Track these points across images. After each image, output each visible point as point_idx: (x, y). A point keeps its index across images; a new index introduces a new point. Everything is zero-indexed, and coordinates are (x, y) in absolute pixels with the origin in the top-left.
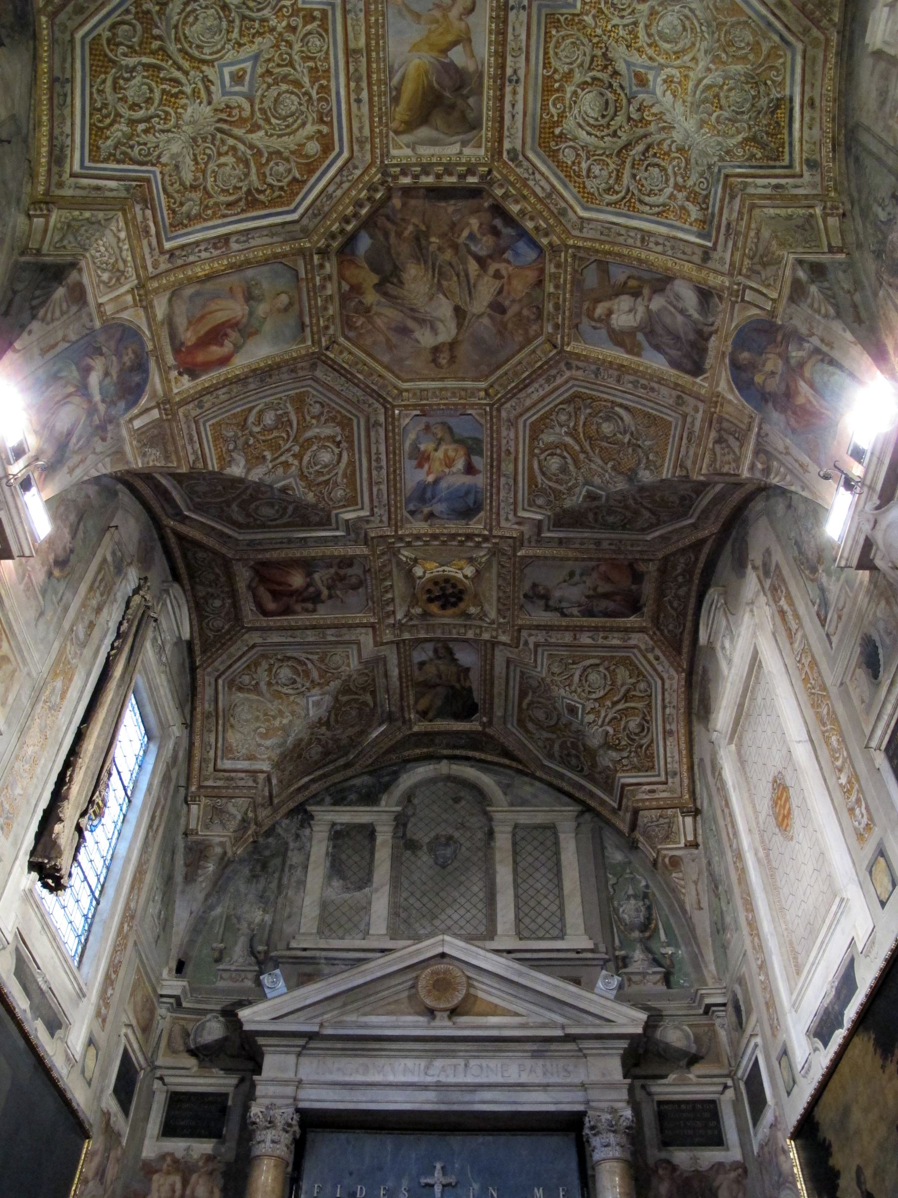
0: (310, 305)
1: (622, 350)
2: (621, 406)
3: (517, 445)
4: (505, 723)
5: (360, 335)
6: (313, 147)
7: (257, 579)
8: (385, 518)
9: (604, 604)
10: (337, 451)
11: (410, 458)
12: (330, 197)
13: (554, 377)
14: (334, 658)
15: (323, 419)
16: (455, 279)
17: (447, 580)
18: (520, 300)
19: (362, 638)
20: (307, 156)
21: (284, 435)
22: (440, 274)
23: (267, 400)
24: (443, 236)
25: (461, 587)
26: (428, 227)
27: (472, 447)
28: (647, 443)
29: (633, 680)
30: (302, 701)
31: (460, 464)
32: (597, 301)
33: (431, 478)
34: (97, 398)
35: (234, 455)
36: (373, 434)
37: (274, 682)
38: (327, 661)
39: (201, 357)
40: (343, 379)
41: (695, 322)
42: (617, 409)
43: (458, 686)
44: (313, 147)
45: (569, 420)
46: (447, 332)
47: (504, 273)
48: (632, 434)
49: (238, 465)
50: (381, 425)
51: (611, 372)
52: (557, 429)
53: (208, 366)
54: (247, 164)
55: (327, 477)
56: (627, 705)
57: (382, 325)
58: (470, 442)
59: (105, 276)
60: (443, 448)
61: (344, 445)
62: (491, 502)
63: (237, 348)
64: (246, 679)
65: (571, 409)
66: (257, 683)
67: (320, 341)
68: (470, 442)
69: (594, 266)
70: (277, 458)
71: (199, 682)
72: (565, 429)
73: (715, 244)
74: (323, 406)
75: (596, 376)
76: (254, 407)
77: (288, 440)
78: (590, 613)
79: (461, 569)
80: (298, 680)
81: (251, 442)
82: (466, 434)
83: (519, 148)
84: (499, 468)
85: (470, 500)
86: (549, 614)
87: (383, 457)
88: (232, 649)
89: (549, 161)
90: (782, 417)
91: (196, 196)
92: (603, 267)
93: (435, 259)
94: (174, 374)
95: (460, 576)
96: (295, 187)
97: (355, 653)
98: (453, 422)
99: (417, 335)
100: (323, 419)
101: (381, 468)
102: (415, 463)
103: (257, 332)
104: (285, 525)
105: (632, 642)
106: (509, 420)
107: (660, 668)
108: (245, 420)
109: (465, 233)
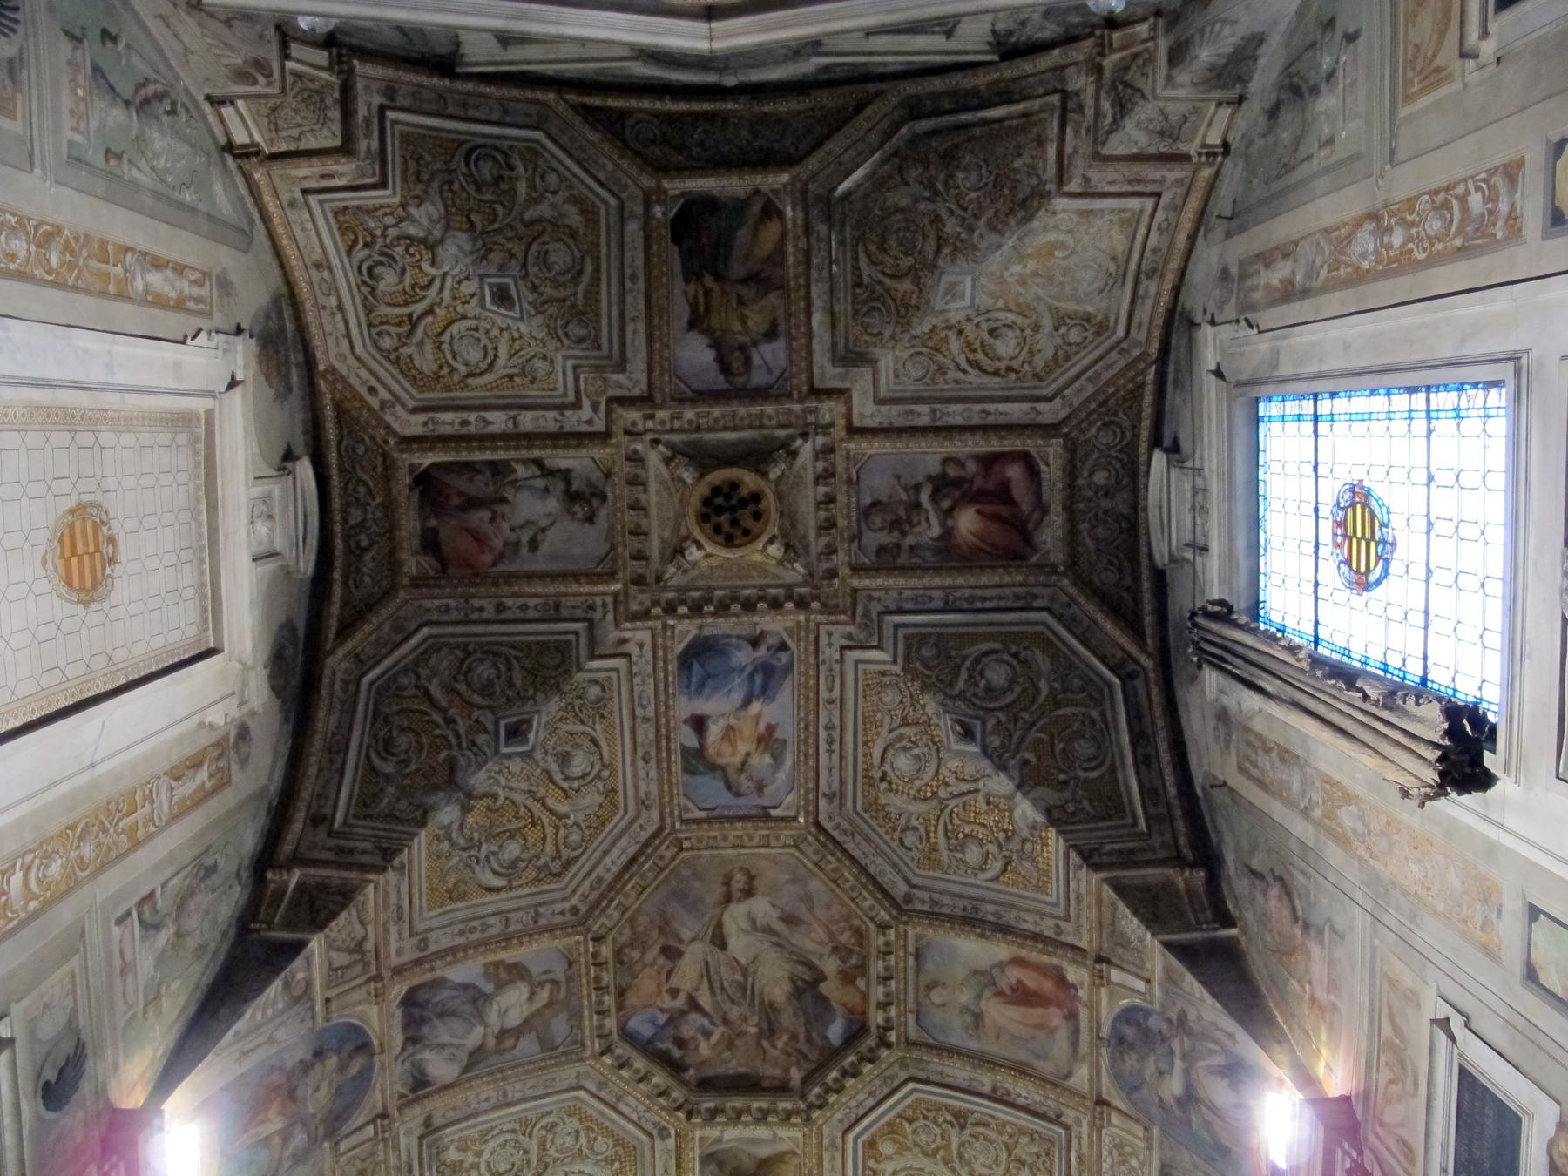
0: (906, 984)
2: (498, 890)
3: (635, 776)
4: (622, 207)
6: (886, 1148)
7: (1030, 526)
8: (824, 640)
9: (480, 486)
10: (887, 767)
11: (785, 742)
12: (872, 1094)
13: (592, 888)
14: (920, 374)
15: (903, 821)
16: (726, 984)
17: (729, 541)
18: (645, 966)
19: (870, 408)
20: (894, 1141)
21: (956, 821)
22: (743, 988)
23: (972, 881)
24: (741, 1034)
25: (708, 527)
26: (759, 1044)
27: (697, 760)
28: (456, 860)
29: (405, 351)
30: (984, 300)
31: (714, 731)
32: (549, 1005)
33: (755, 707)
34: (1178, 1063)
35: (1026, 833)
36: (836, 784)
37: (1028, 332)
38: (934, 367)
39: (1048, 986)
40: (872, 870)
41: (425, 1047)
42: (501, 882)
43: (709, 281)
44: (886, 1148)
45: (566, 837)
46: (735, 917)
47: (666, 997)
48: (478, 862)
49: (1024, 816)
50: (825, 795)
52: (581, 818)
53: (1041, 969)
54: (960, 1156)
55: (905, 731)
56: (405, 310)
58: (701, 768)
59: (1134, 1162)
60: (737, 759)
61: (877, 775)
62: (666, 678)
63: (1001, 966)
64: (1075, 336)
65: (566, 853)
66: (1057, 329)
67: (898, 936)
68: (701, 768)
69: (558, 1041)
70: (970, 792)
71: (1157, 333)
72: (570, 822)
73: (420, 1145)
74: (901, 841)
76: (991, 880)
77: (952, 812)
78: (499, 470)
79: (708, 556)
80: (985, 336)
81: (1001, 836)
83: (658, 1143)
84: (658, 730)
85: (696, 667)
86: (563, 464)
87: (823, 746)
88: (1091, 389)
89: (622, 1134)
90: (289, 1065)
91: (1018, 1152)
92: (547, 1045)
93: (752, 1004)
94: (1082, 993)
95: (710, 548)
96: (910, 1113)
97: (883, 380)
98: (725, 798)
99: (775, 914)
100: (903, 821)
101: (827, 728)
102: (778, 734)
103: (975, 973)
104: (975, 639)
105: (422, 417)
106: (648, 807)
107: (364, 374)
108: (1005, 870)
109: (715, 1037)
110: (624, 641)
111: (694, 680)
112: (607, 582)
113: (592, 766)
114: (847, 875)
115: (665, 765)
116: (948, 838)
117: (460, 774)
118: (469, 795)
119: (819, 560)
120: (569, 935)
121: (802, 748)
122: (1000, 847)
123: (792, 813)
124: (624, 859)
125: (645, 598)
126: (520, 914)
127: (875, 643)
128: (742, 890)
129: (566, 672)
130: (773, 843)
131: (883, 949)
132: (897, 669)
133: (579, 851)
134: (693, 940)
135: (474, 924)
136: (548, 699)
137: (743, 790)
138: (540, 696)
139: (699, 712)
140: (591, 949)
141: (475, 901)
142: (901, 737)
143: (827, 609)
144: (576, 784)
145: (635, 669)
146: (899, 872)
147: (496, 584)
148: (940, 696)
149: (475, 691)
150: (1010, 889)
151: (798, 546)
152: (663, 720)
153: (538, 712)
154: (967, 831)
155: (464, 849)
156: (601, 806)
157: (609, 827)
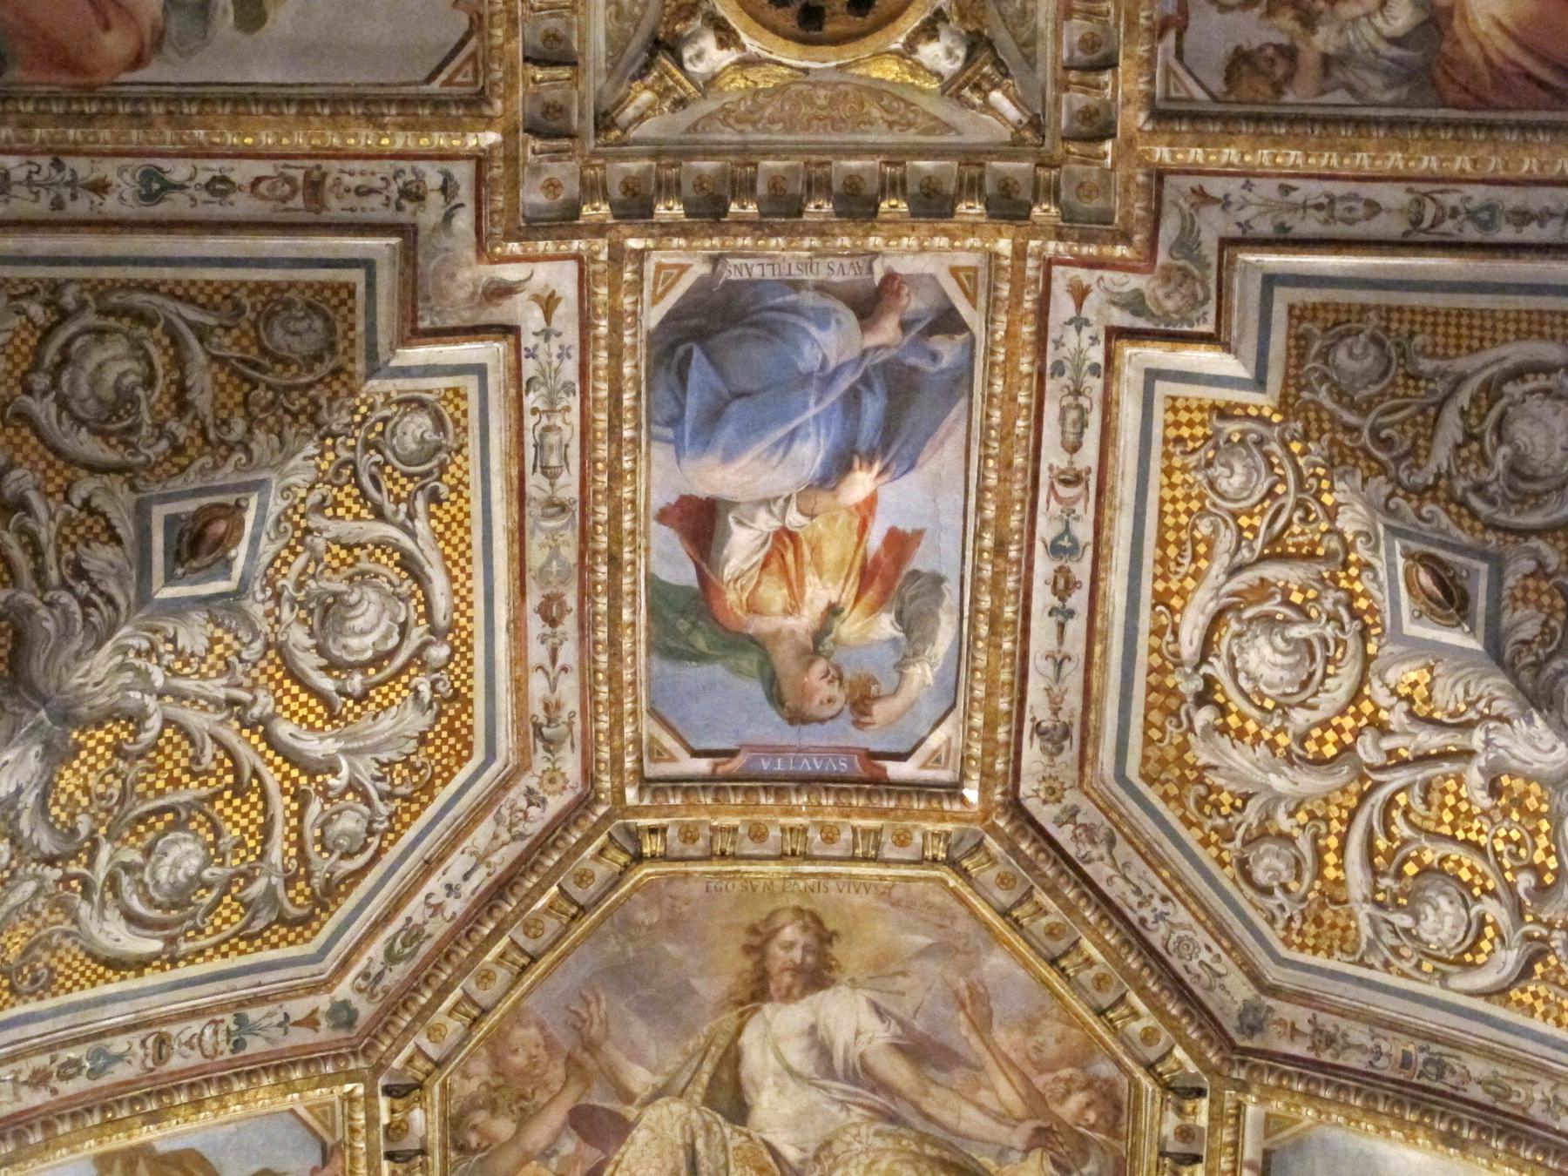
1: (162, 1147)
2: (140, 964)
3: (519, 658)
5: (1080, 1059)
8: (1062, 306)
10: (1218, 668)
11: (938, 580)
13: (391, 957)
15: (1252, 814)
18: (526, 1159)
21: (1401, 829)
23: (1434, 991)
33: (861, 483)
36: (1074, 701)
40: (1156, 940)
42: (156, 945)
45: (326, 823)
48: (87, 887)
50: (1037, 727)
51: (195, 1058)
52: (366, 769)
55: (1271, 572)
57: (1002, 1084)
60: (805, 621)
65: (322, 864)
67: (1216, 1119)
68: (701, 643)
70: (1444, 755)
75: (240, 1020)
76: (1487, 995)
77: (1390, 803)
81: (1525, 881)
82: (717, 671)
85: (699, 371)
87: (1042, 598)
95: (753, 45)
98: (768, 727)
99: (878, 1034)
100: (1252, 814)
101: (1055, 549)
102: (921, 561)
106: (551, 745)
108: (1526, 972)
110: (505, 291)
111: (692, 401)
112: (458, 127)
113: (404, 629)
114: (1088, 947)
115: (602, 634)
116: (1376, 873)
117: (36, 667)
118: (67, 717)
119: (1064, 86)
120: (324, 1081)
121: (986, 602)
122: (1518, 910)
123: (945, 775)
124: (480, 879)
125: (565, 172)
126: (195, 1026)
127: (1208, 327)
128: (797, 970)
129: (336, 372)
130: (889, 852)
131: (1174, 1146)
132: (1264, 402)
133: (361, 860)
134: (659, 1093)
135: (72, 1054)
136: (285, 451)
137: (813, 707)
138: (262, 442)
139: (702, 491)
140: (385, 1119)
141: (77, 996)
142: (1263, 589)
143: (1075, 225)
144: (356, 682)
145: (529, 368)
146: (1234, 947)
147: (140, 119)
148: (1380, 486)
149: (80, 422)
150: (1536, 1024)
151: (1002, 37)
152: (603, 513)
153: (260, 486)
154: (1428, 857)
155: (51, 861)
156: (423, 740)
157: (444, 794)
